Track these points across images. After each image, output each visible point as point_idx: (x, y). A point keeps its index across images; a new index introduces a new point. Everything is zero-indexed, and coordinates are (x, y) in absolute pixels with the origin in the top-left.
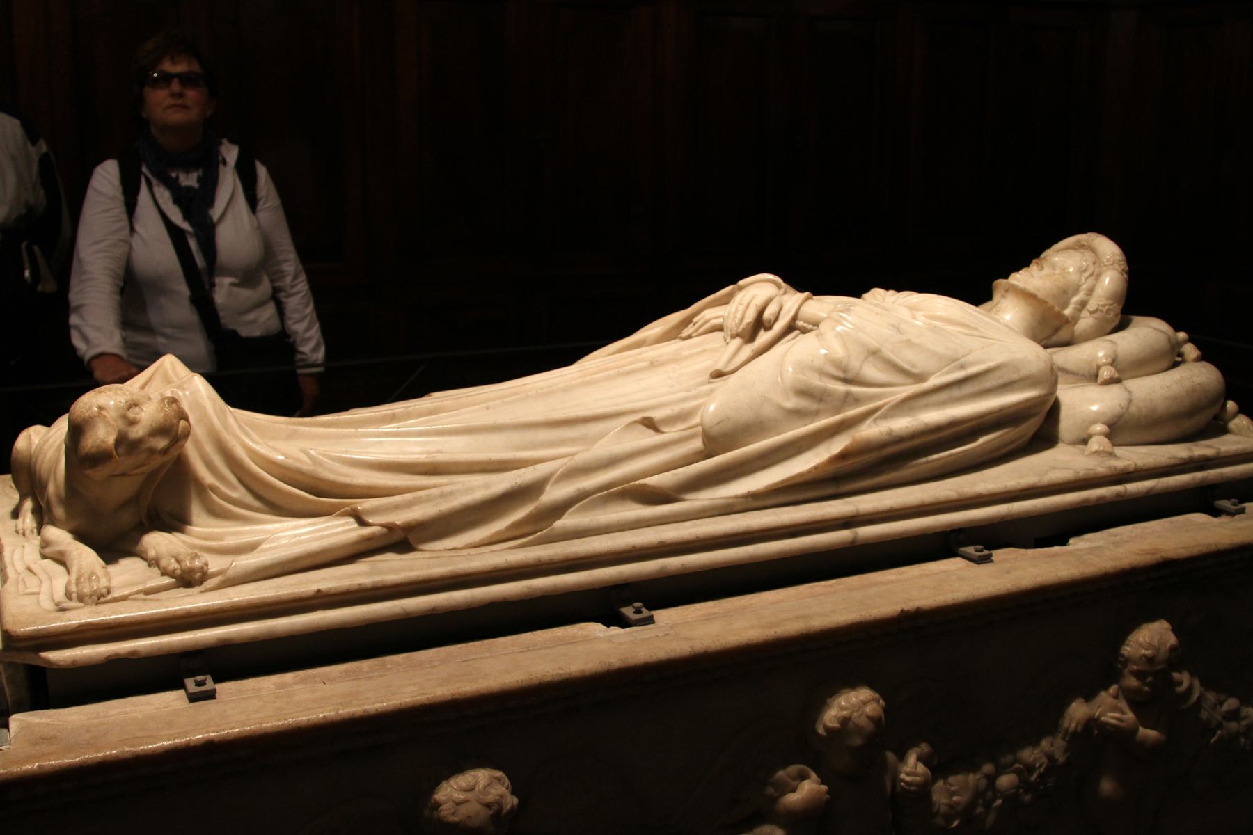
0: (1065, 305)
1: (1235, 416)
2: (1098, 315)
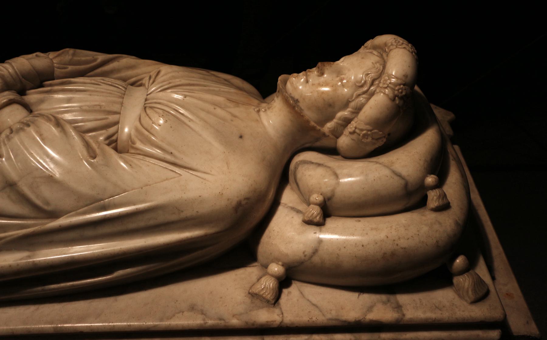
0: (330, 118)
2: (354, 136)
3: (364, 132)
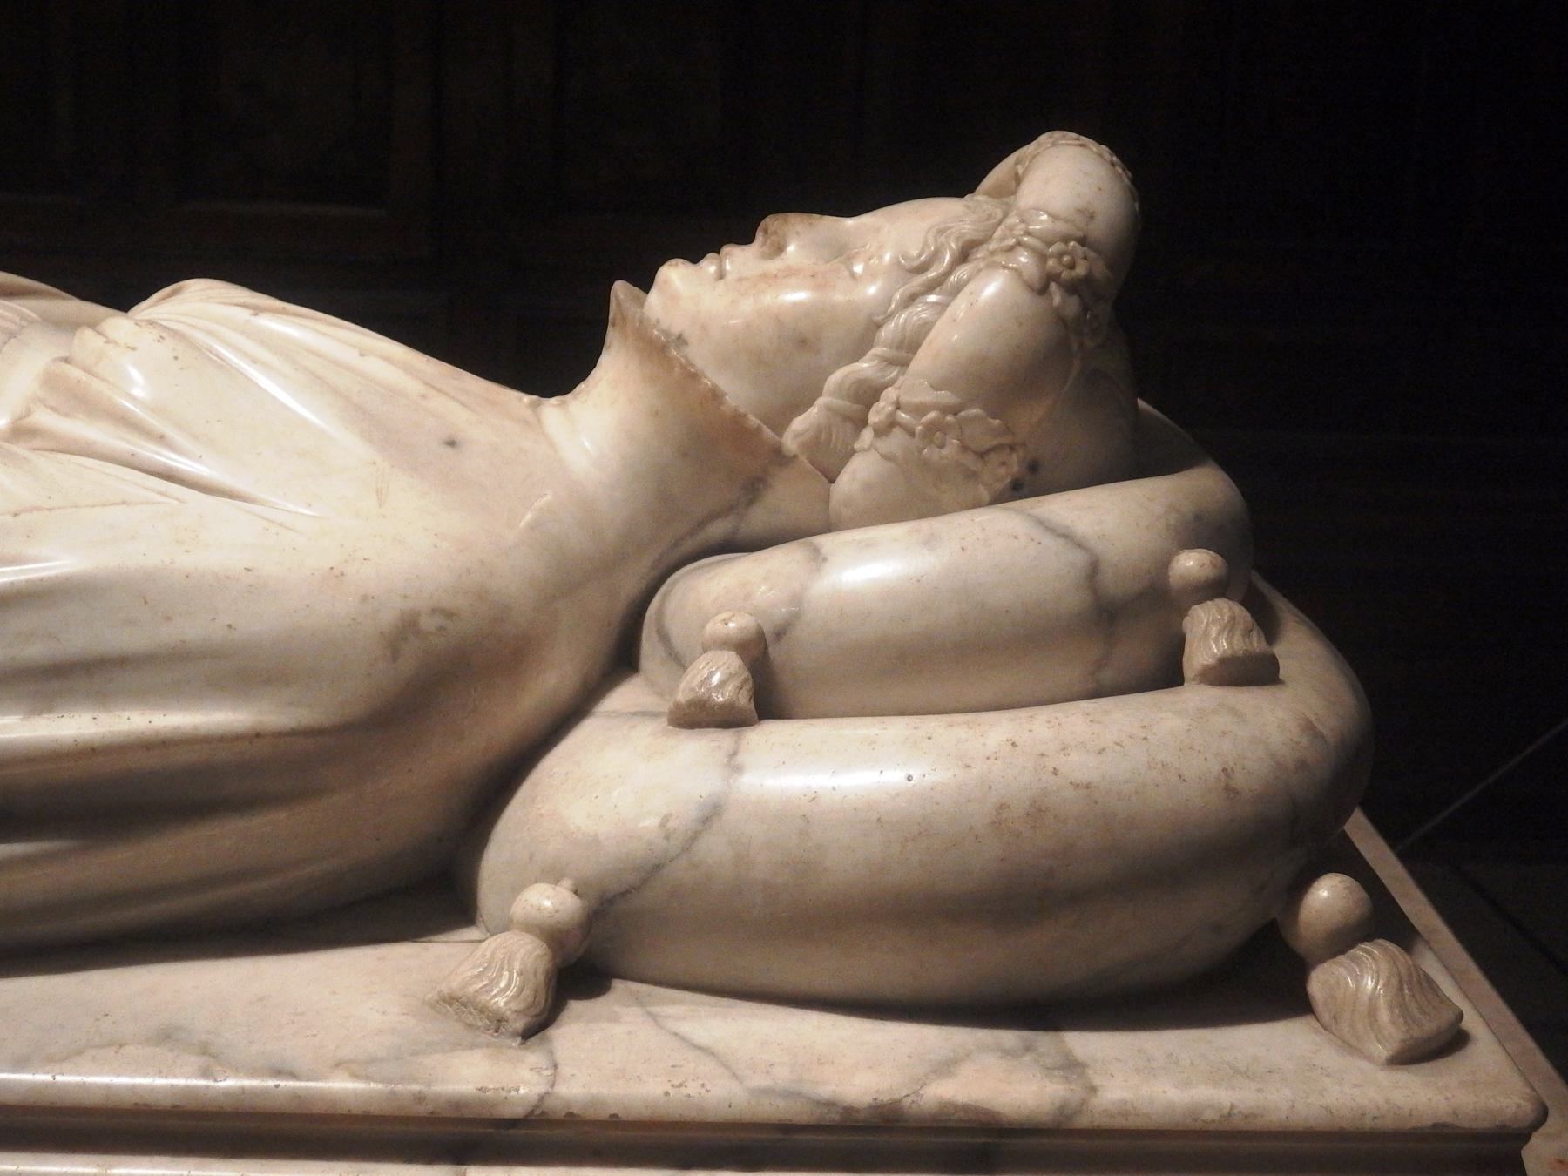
1: (1343, 940)
2: (895, 442)
3: (932, 415)
